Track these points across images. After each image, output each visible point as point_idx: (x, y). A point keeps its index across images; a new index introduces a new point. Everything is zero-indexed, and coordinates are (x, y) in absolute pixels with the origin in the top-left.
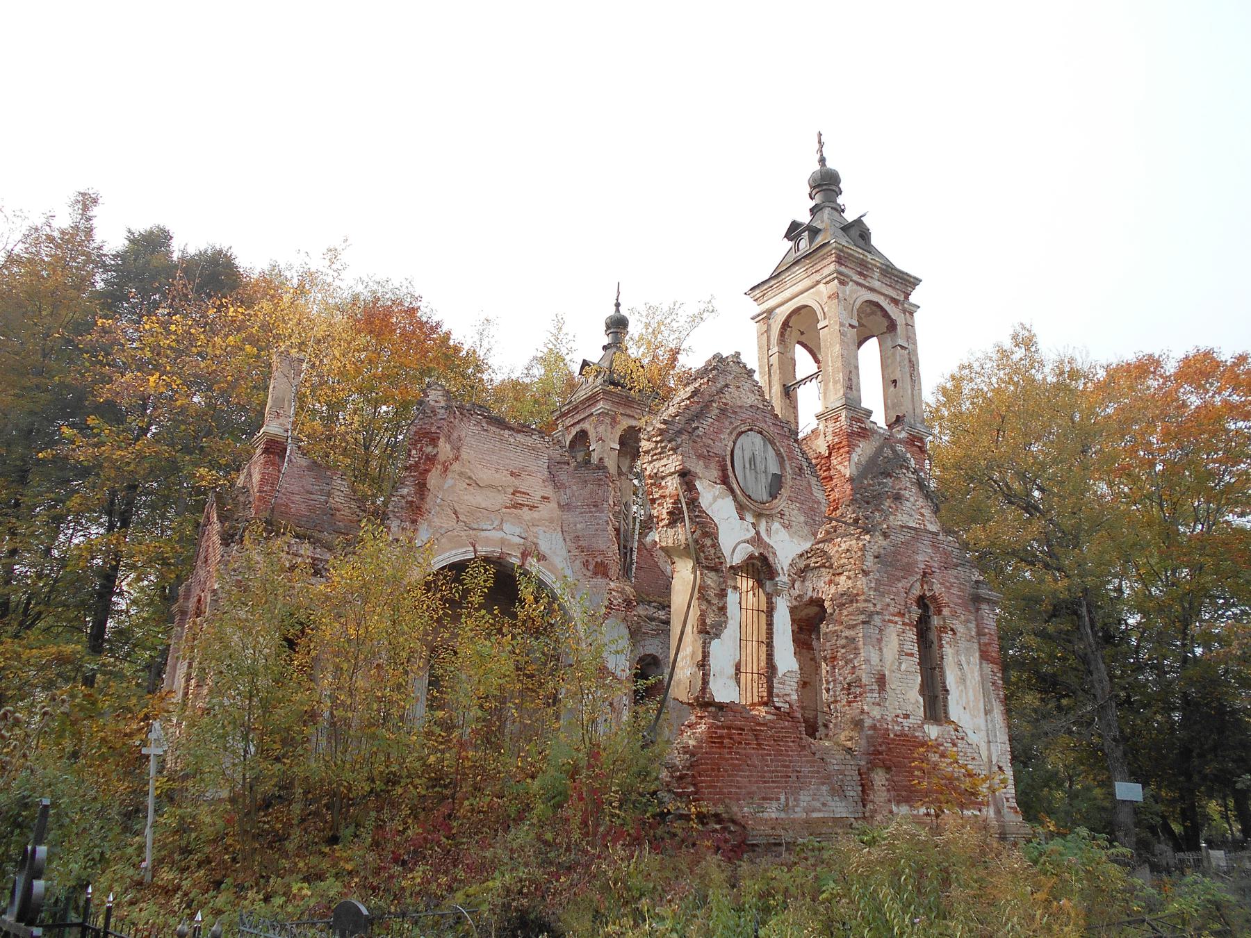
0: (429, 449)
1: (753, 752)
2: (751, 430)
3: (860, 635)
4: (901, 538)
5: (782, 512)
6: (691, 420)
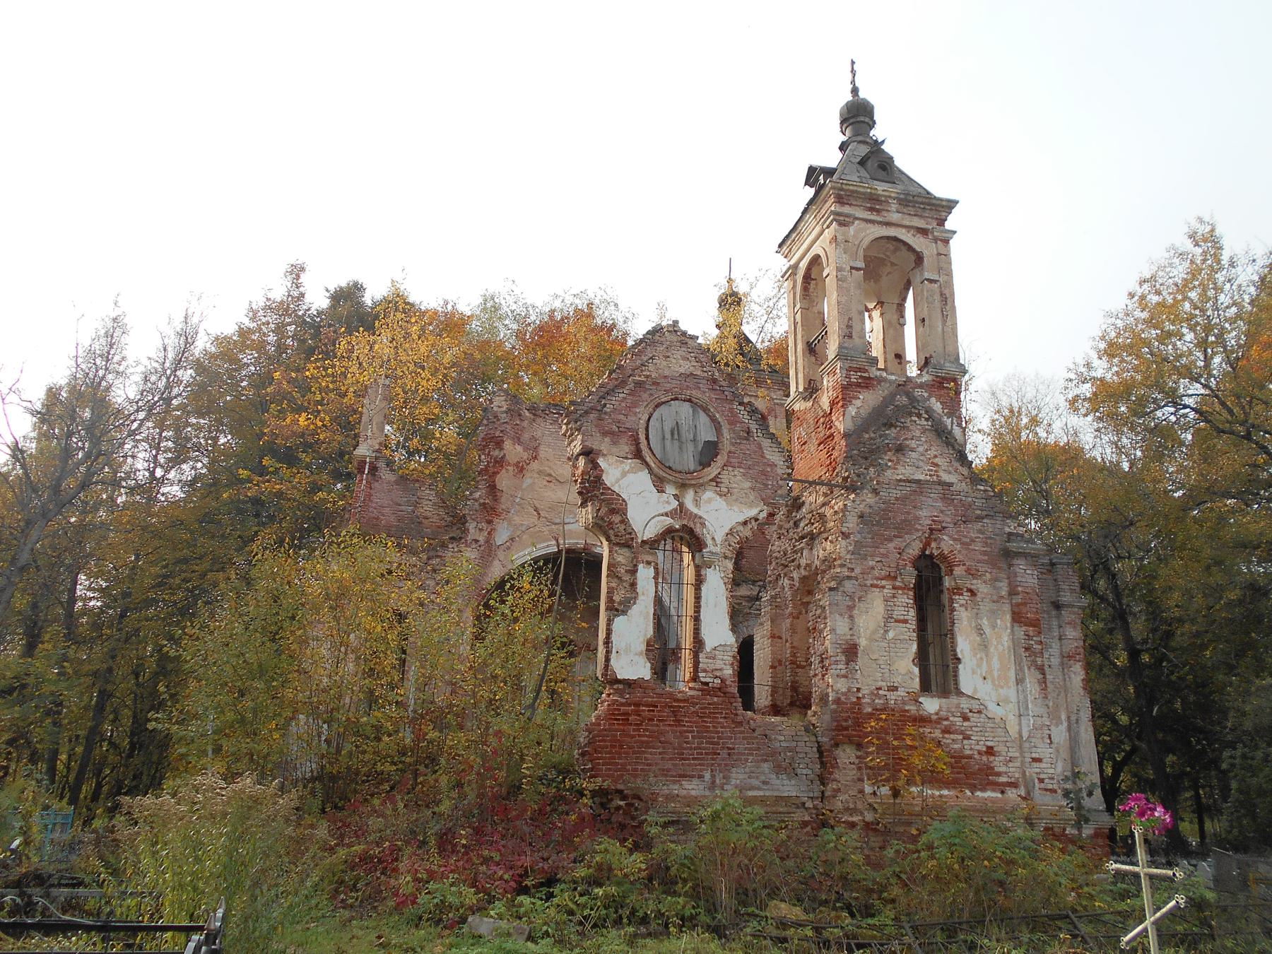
0: (496, 453)
2: (676, 399)
5: (719, 480)
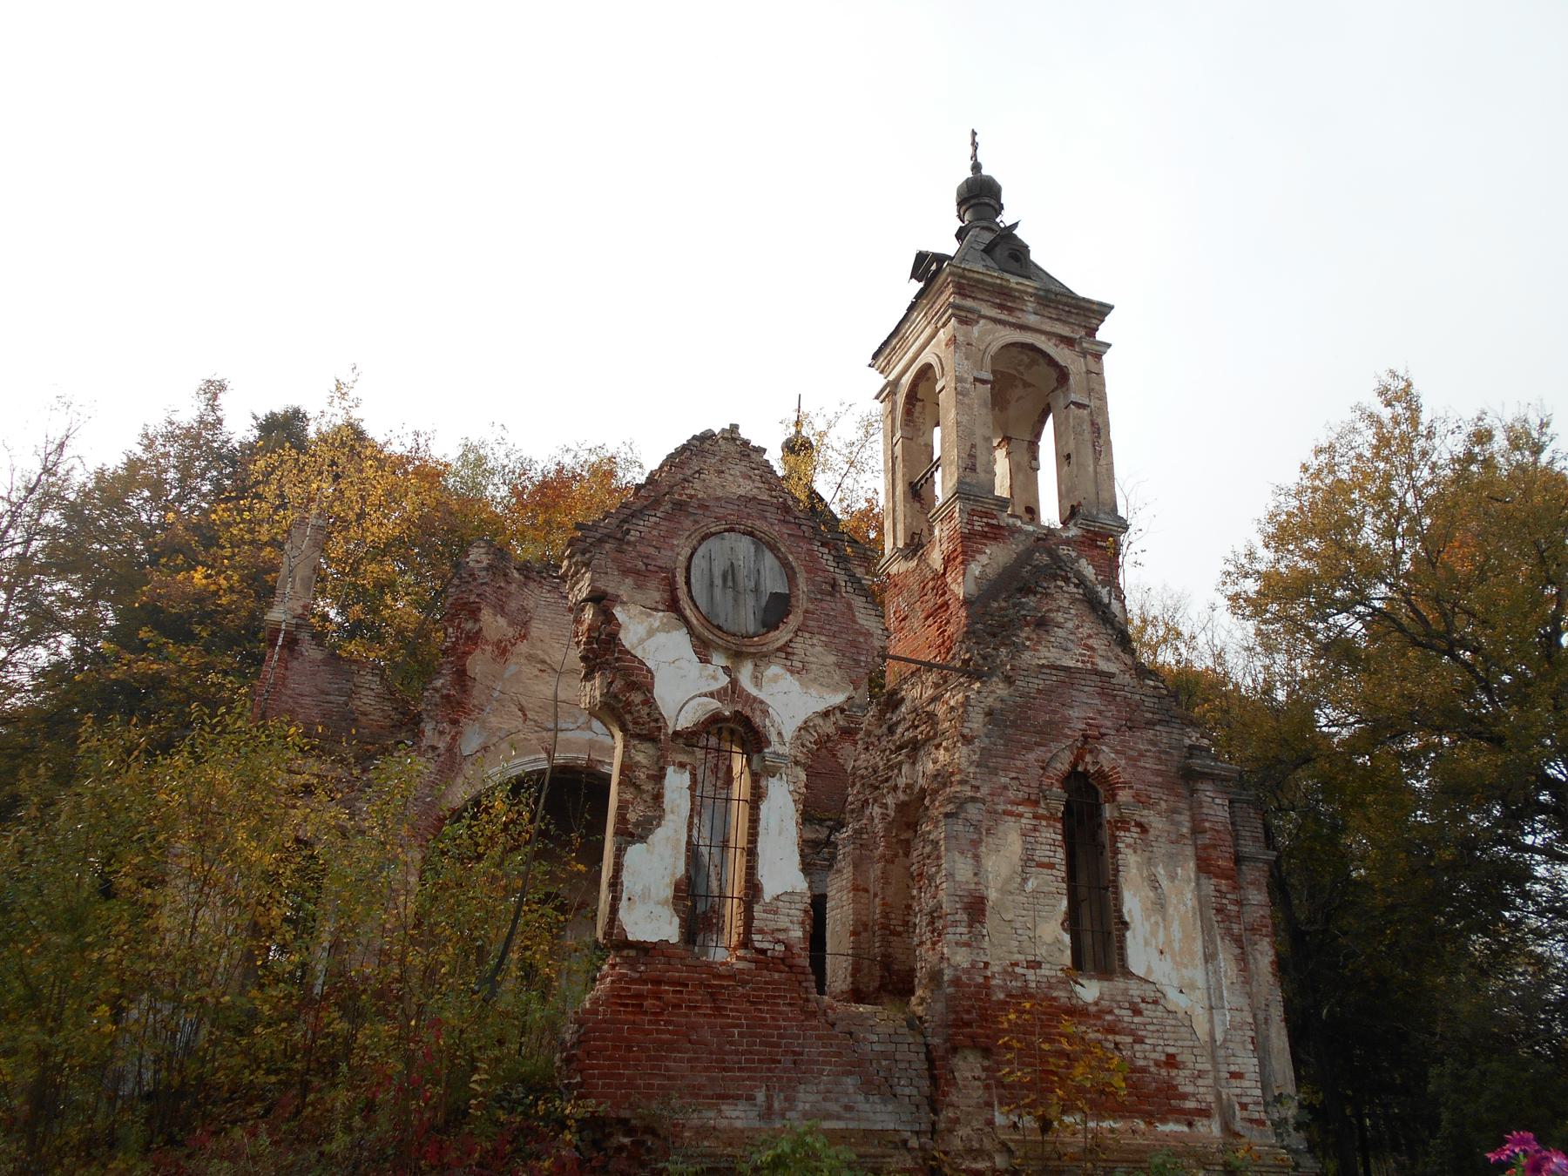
0: (469, 625)
1: (702, 1020)
2: (731, 530)
3: (943, 835)
4: (1037, 683)
5: (789, 650)
6: (625, 521)
